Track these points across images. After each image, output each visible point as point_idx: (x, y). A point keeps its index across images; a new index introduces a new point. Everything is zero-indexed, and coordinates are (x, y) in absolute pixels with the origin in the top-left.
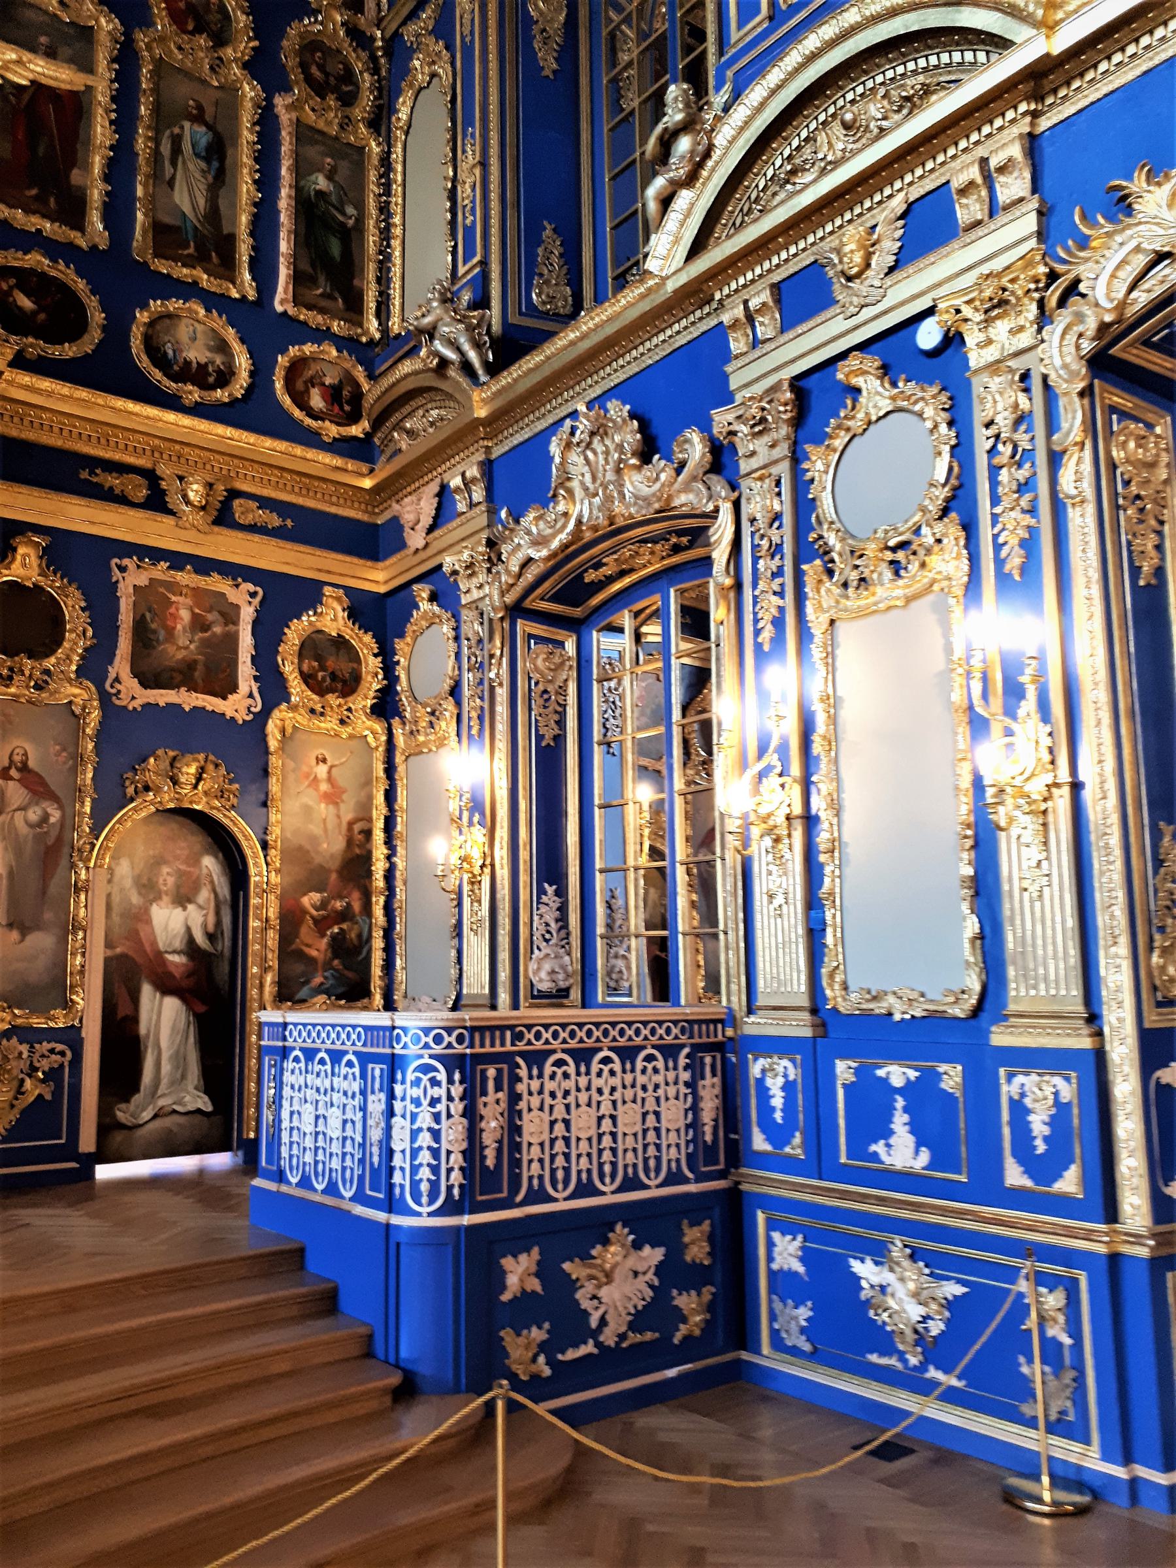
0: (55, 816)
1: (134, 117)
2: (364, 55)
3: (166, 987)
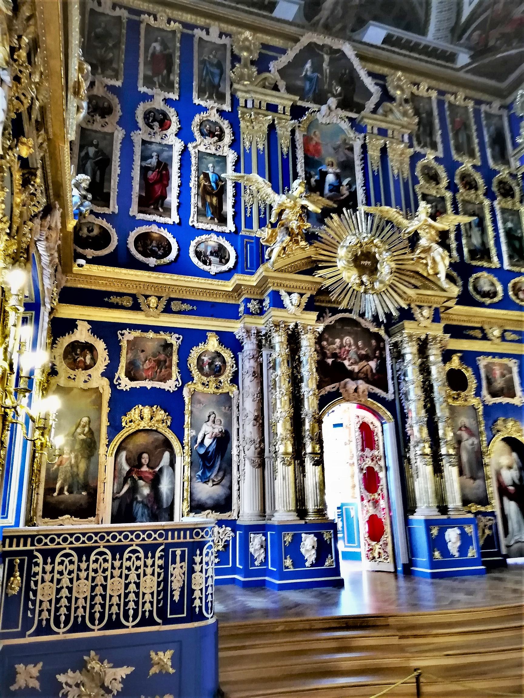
0: (476, 442)
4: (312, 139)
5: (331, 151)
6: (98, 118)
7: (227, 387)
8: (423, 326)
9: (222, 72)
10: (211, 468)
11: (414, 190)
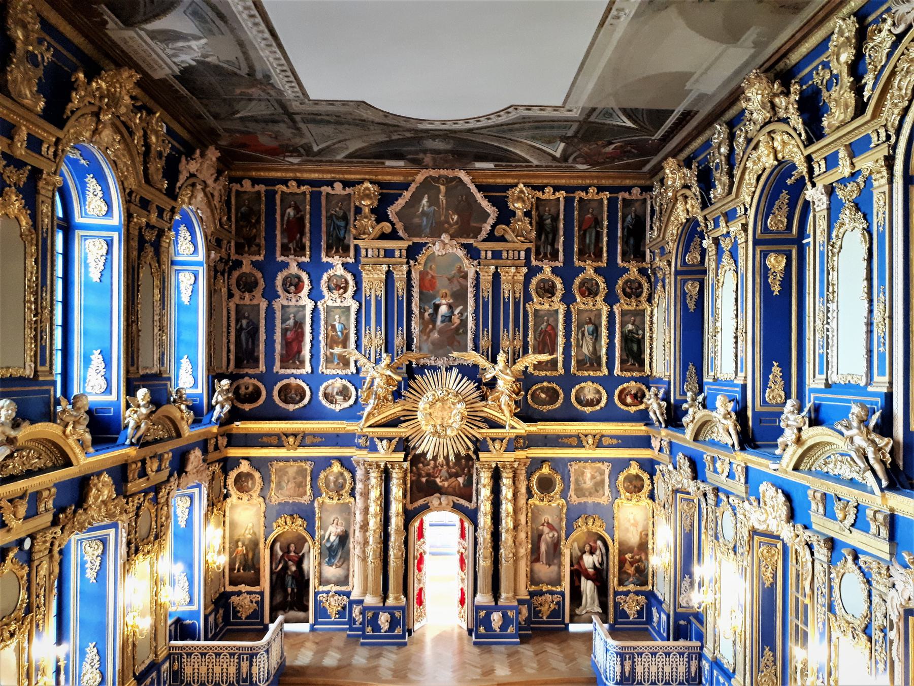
0: (556, 535)
1: (571, 331)
2: (645, 278)
3: (588, 577)
4: (428, 273)
6: (247, 295)
7: (348, 499)
8: (494, 456)
9: (347, 224)
10: (334, 557)
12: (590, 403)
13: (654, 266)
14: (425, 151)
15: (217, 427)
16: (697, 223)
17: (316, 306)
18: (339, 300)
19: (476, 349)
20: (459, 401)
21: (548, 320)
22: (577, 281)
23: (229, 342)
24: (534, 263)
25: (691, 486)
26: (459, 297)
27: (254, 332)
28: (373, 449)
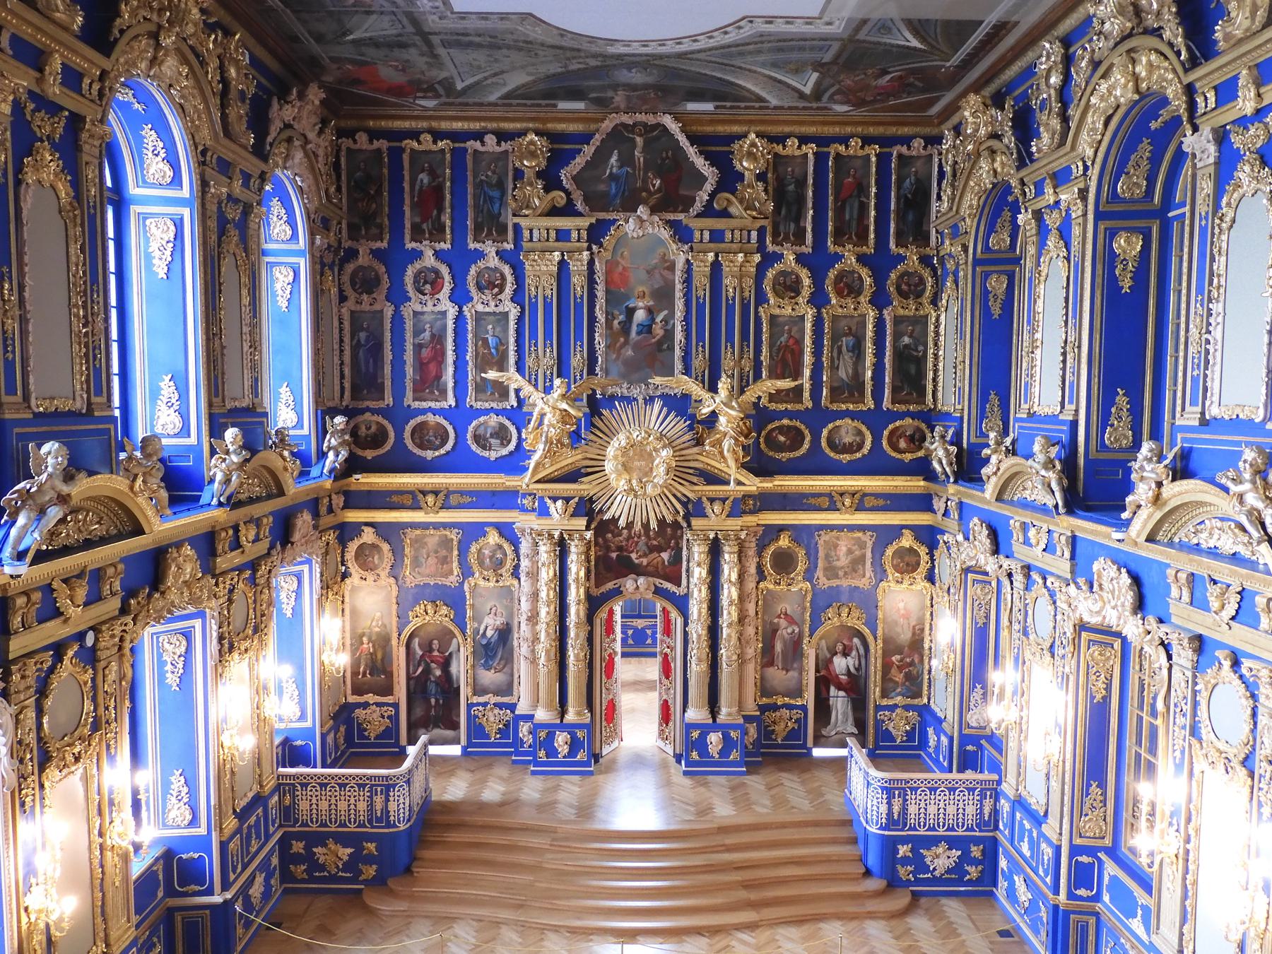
0: (797, 630)
1: (823, 346)
3: (840, 687)
4: (618, 263)
5: (642, 275)
6: (365, 297)
8: (715, 520)
9: (503, 192)
10: (493, 657)
11: (756, 312)
12: (848, 449)
13: (942, 254)
14: (615, 87)
15: (330, 481)
16: (1008, 189)
17: (460, 311)
18: (492, 304)
19: (687, 371)
20: (664, 447)
21: (790, 331)
22: (832, 274)
23: (342, 364)
24: (771, 248)
25: (990, 564)
26: (663, 296)
27: (376, 349)
28: (544, 512)
